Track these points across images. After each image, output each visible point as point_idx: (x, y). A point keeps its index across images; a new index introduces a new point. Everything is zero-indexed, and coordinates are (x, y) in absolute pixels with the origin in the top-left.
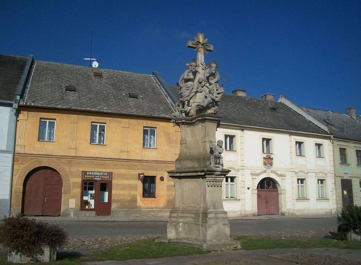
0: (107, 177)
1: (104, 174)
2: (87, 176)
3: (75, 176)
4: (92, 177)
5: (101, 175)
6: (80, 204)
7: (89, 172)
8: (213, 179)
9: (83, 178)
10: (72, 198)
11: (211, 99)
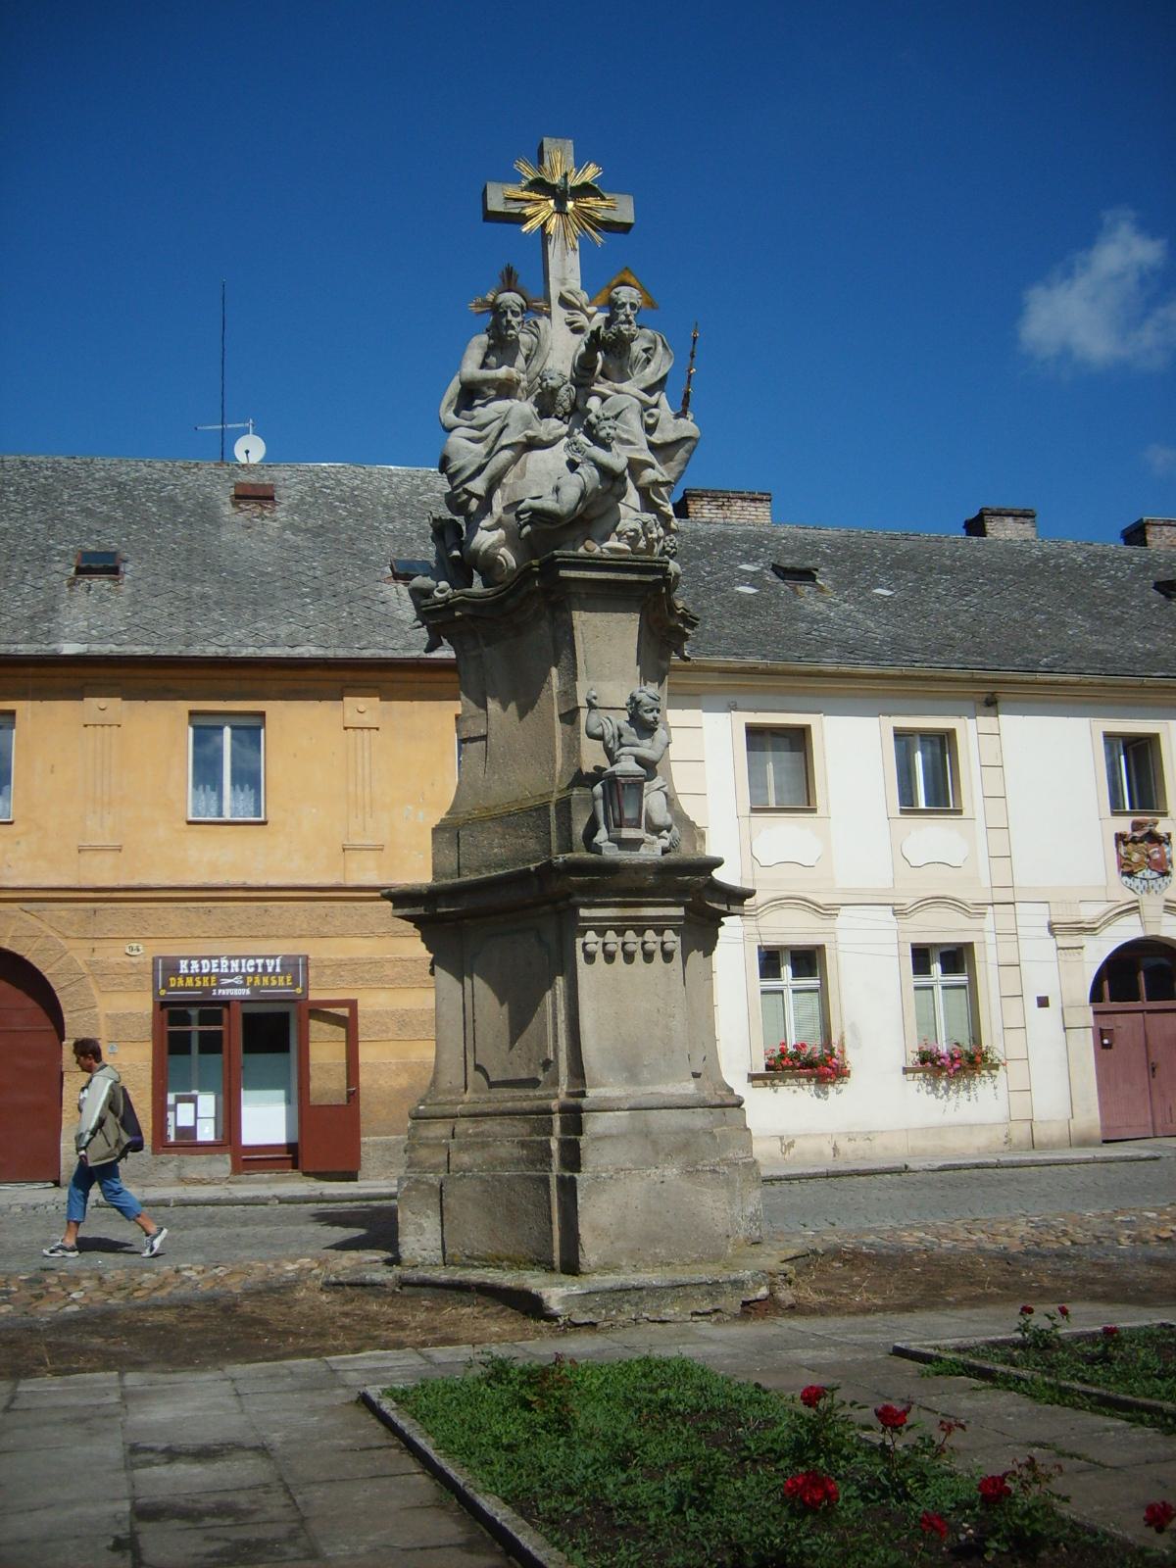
0: (281, 979)
1: (264, 966)
2: (181, 982)
3: (122, 984)
4: (206, 983)
5: (251, 970)
6: (150, 1120)
7: (190, 958)
9: (163, 992)
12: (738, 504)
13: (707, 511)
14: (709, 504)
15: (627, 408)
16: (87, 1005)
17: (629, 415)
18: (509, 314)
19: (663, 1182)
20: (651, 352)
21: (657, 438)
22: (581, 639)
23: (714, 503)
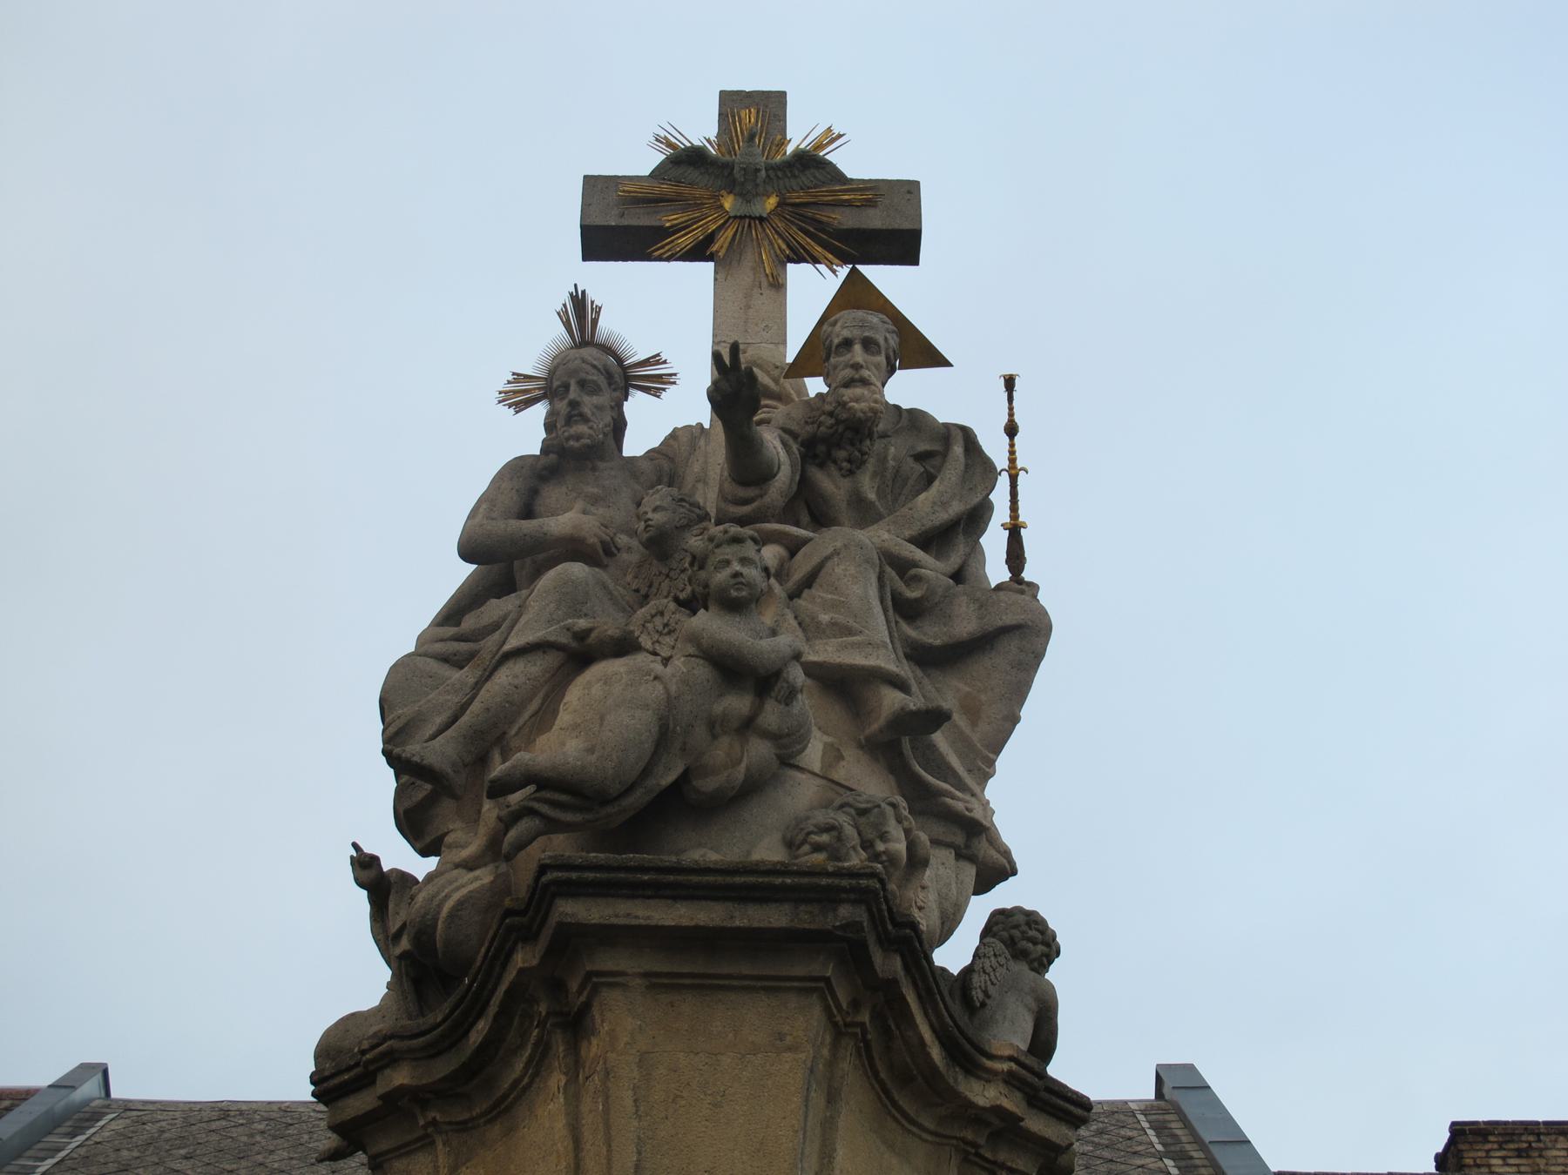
11: (702, 672)
12: (1559, 1146)
13: (1500, 1162)
14: (1501, 1148)
15: (836, 553)
17: (839, 570)
18: (573, 387)
20: (936, 461)
21: (931, 634)
22: (629, 1102)
23: (1512, 1146)
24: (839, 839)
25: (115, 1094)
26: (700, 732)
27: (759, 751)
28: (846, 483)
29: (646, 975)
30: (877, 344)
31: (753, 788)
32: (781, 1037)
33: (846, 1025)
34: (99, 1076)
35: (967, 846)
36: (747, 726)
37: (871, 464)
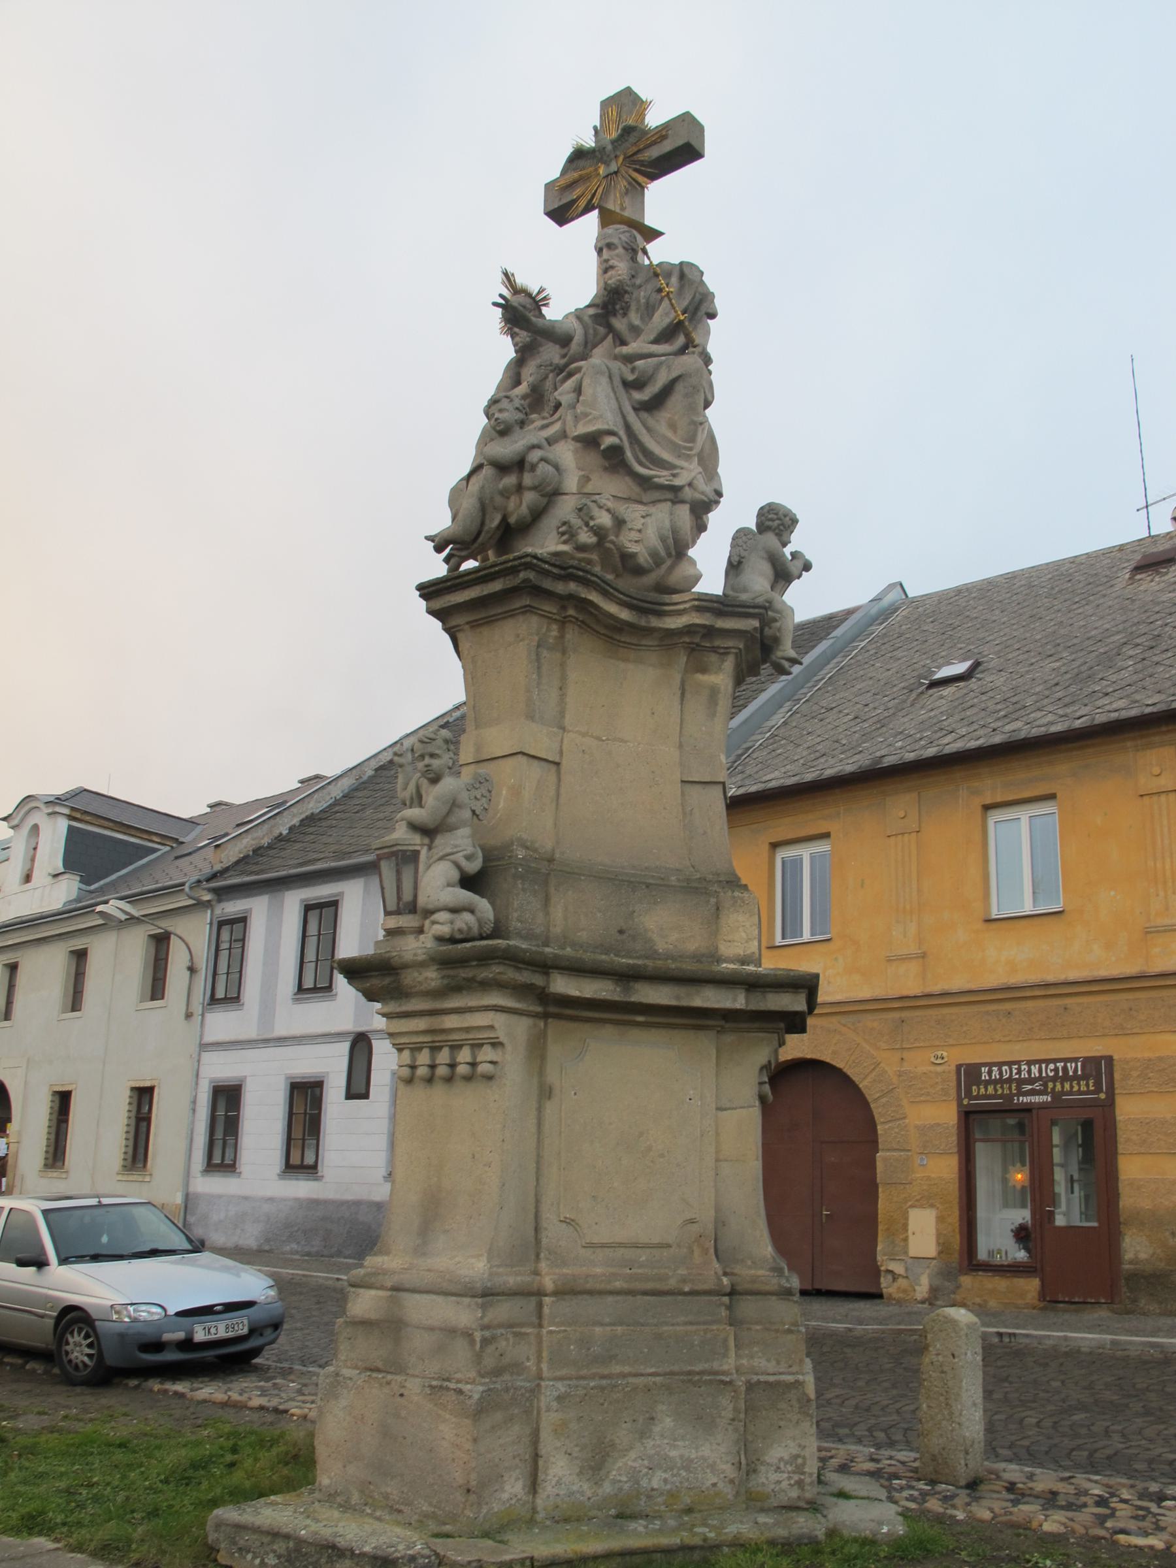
0: (1083, 1083)
1: (1065, 1069)
2: (982, 1091)
3: (928, 1094)
4: (1006, 1091)
5: (1051, 1074)
6: (958, 1237)
7: (990, 1065)
8: (421, 1024)
9: (965, 1102)
10: (922, 1207)
16: (898, 1116)
19: (402, 1395)
24: (570, 527)
25: (910, 595)
26: (499, 500)
27: (529, 497)
28: (625, 320)
29: (468, 623)
30: (613, 244)
31: (538, 514)
32: (518, 636)
33: (565, 617)
34: (899, 586)
35: (676, 497)
36: (519, 488)
37: (633, 307)
